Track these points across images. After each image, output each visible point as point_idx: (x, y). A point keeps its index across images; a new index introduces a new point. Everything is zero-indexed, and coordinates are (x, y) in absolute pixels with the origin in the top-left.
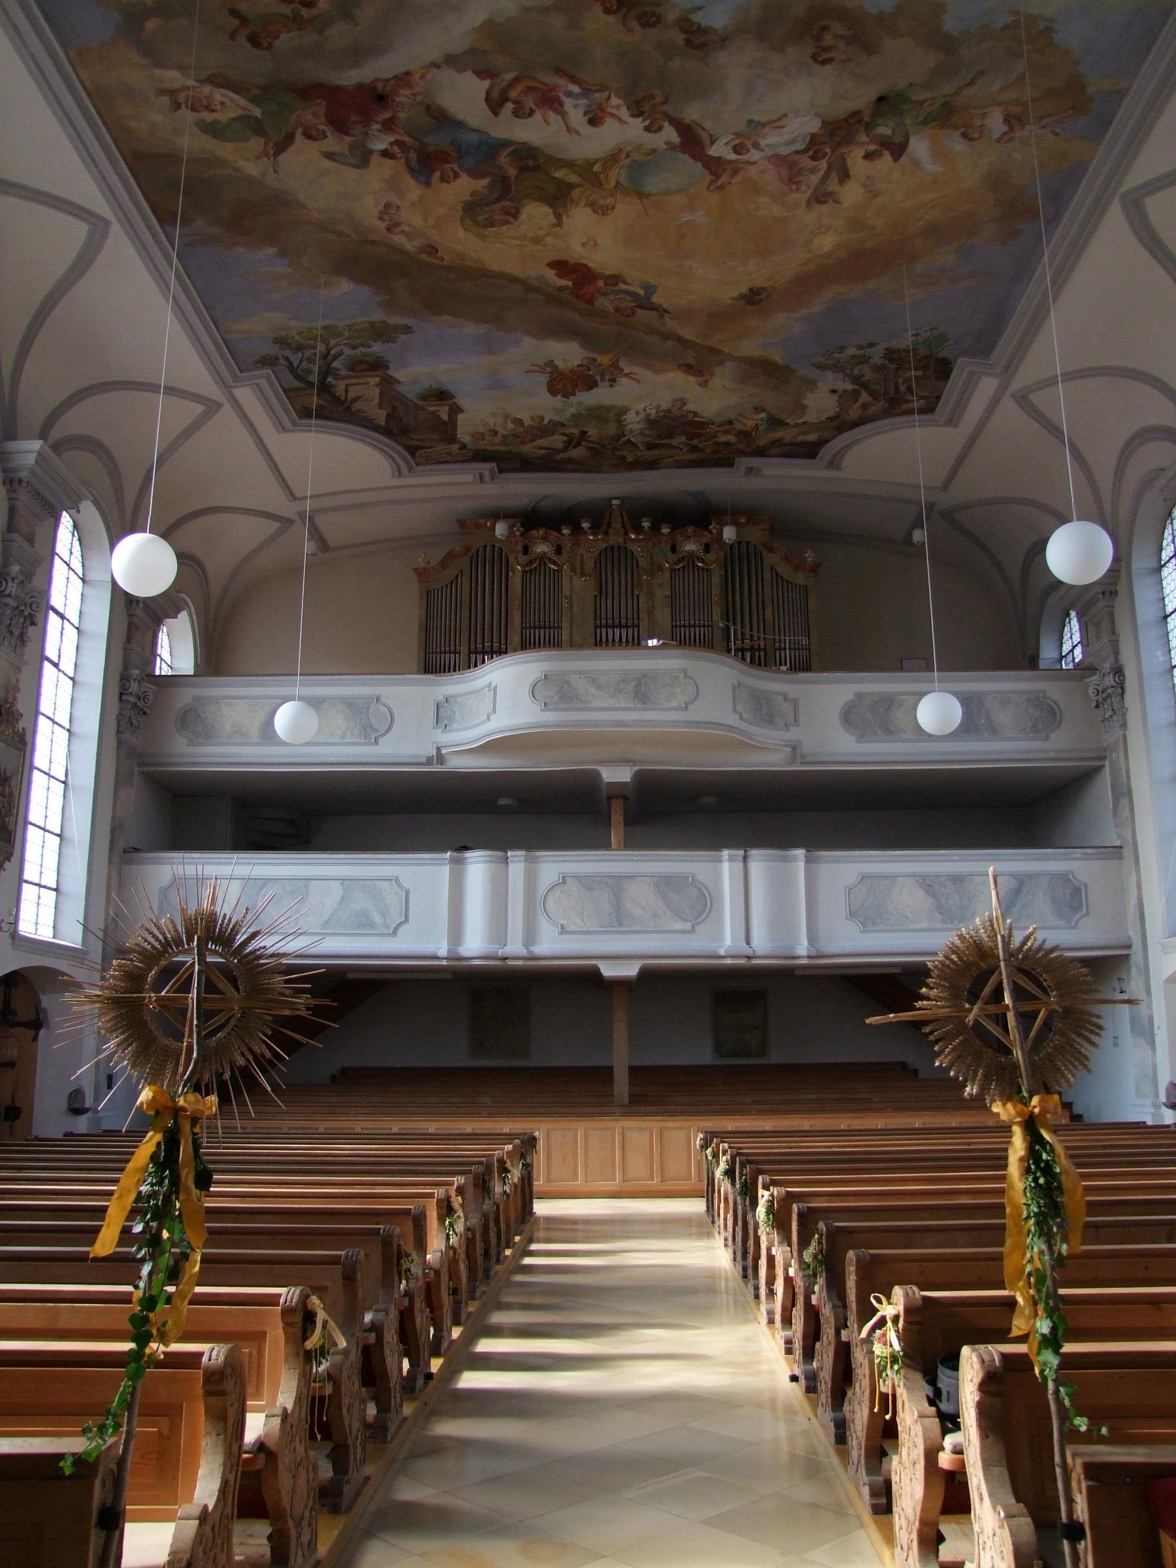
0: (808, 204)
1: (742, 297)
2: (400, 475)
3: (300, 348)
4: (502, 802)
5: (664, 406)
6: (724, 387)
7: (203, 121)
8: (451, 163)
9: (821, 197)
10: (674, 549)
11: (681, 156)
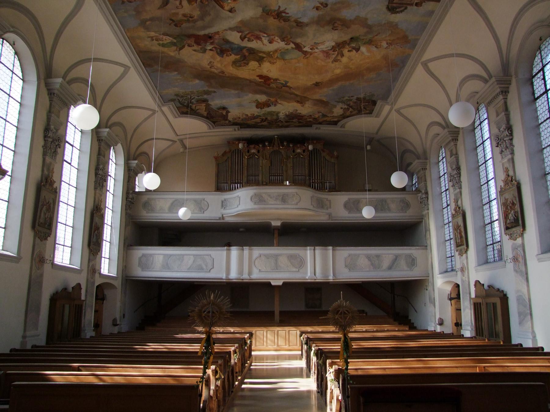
0: (332, 62)
1: (313, 84)
2: (210, 129)
3: (182, 97)
4: (241, 230)
5: (291, 111)
9: (335, 60)
10: (294, 151)
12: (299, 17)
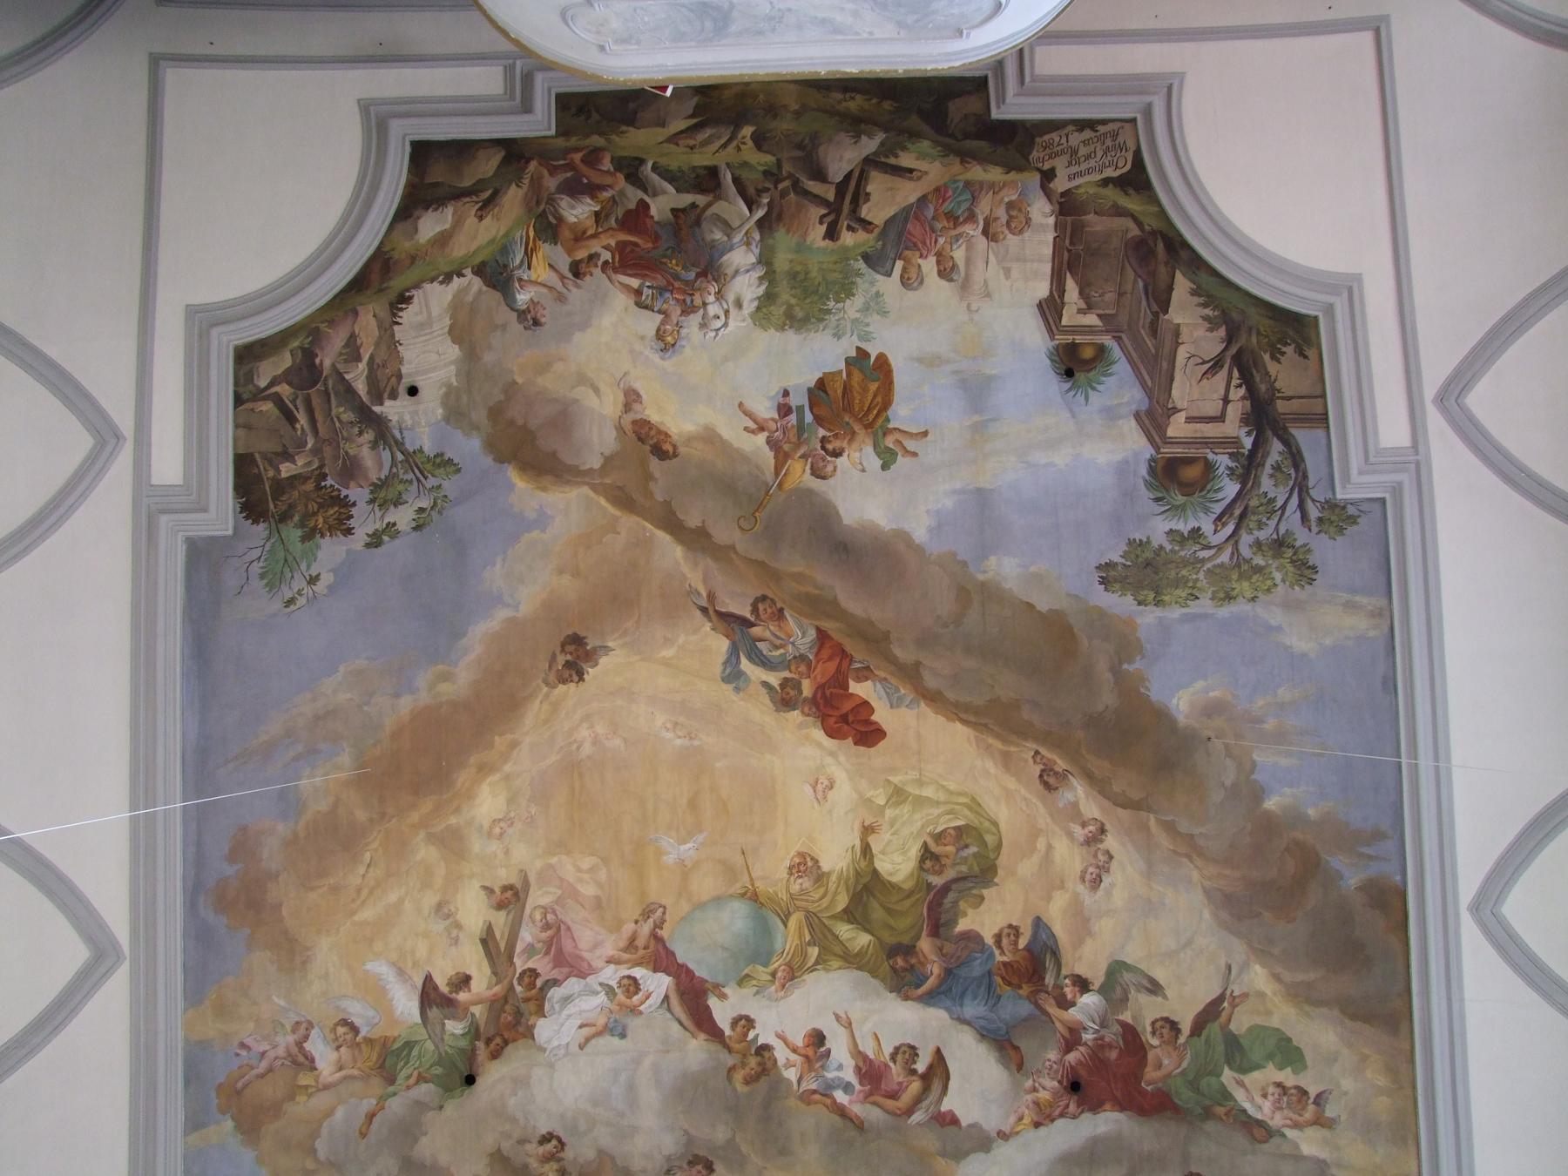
1: (591, 656)
6: (596, 390)
7: (1295, 1072)
8: (1005, 964)
9: (511, 897)
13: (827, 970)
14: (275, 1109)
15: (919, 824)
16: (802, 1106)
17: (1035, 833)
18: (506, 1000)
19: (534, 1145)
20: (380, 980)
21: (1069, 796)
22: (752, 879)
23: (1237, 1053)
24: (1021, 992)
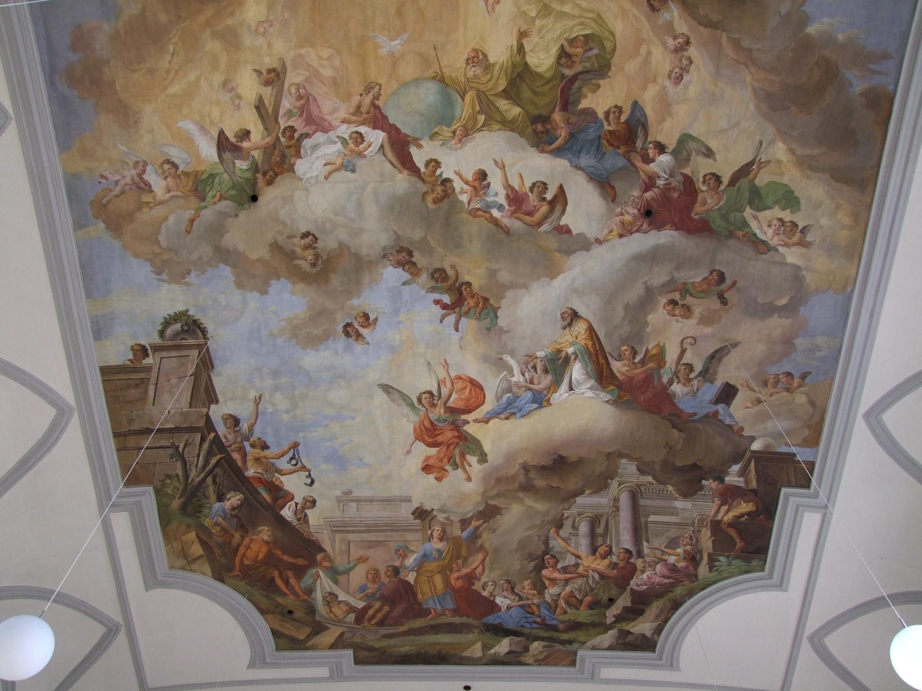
7: (792, 212)
8: (609, 131)
11: (408, 133)
12: (406, 289)
13: (490, 131)
14: (130, 217)
15: (559, 31)
16: (471, 218)
17: (640, 42)
18: (275, 148)
19: (298, 239)
20: (189, 133)
21: (667, 16)
22: (440, 67)
23: (757, 199)
24: (619, 151)
